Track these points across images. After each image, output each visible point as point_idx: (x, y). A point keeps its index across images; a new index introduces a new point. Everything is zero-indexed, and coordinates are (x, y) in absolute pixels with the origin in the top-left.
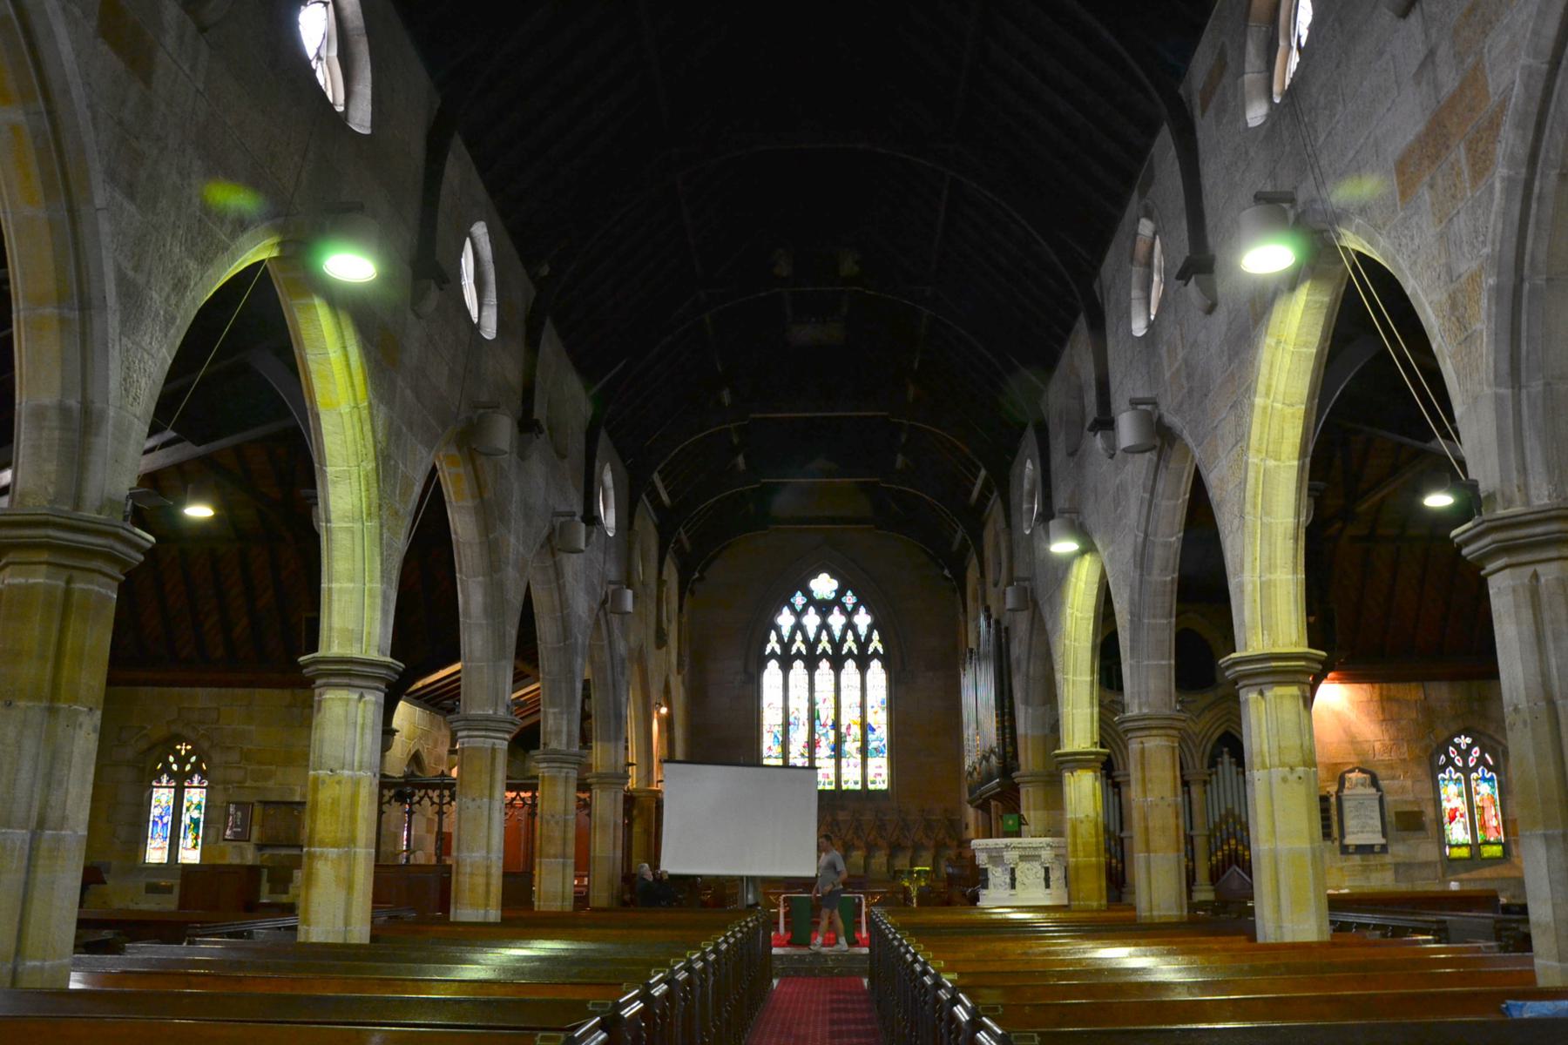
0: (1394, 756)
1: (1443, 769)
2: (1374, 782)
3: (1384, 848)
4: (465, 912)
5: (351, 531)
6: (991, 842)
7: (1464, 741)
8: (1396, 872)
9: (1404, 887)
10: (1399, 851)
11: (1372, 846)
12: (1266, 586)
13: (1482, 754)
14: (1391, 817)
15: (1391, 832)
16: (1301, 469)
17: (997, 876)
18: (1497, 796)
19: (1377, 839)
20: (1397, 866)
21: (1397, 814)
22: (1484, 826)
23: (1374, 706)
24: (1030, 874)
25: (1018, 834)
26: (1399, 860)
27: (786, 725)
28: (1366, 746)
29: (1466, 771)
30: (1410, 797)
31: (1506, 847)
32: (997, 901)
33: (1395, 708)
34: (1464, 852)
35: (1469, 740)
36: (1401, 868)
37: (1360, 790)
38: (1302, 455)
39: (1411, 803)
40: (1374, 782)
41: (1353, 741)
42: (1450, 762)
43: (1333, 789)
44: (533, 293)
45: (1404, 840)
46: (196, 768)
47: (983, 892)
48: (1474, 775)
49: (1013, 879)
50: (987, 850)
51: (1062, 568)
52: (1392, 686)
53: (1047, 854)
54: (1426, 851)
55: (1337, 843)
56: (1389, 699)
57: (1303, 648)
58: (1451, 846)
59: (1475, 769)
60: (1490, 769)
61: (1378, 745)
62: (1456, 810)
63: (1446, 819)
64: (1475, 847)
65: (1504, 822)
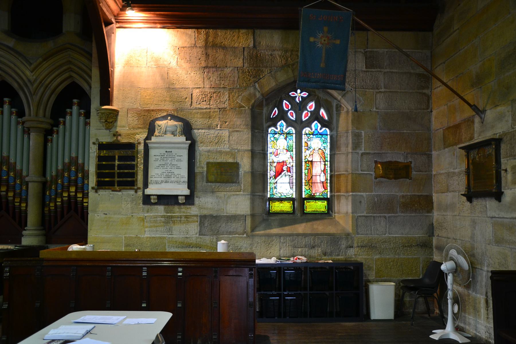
0: (213, 104)
2: (187, 130)
3: (189, 200)
7: (299, 95)
8: (201, 224)
11: (176, 196)
13: (317, 109)
15: (200, 183)
18: (328, 152)
19: (183, 190)
20: (203, 218)
21: (208, 163)
22: (311, 182)
23: (198, 52)
26: (205, 212)
28: (184, 94)
29: (299, 125)
30: (225, 148)
31: (329, 201)
33: (220, 54)
34: (286, 207)
35: (305, 94)
36: (210, 222)
37: (169, 138)
39: (227, 153)
41: (170, 87)
42: (282, 115)
43: (141, 136)
45: (213, 192)
48: (307, 130)
52: (220, 33)
55: (140, 193)
56: (215, 46)
58: (272, 199)
59: (308, 124)
60: (324, 123)
61: (196, 93)
62: (284, 163)
63: (271, 173)
64: (299, 202)
65: (331, 177)
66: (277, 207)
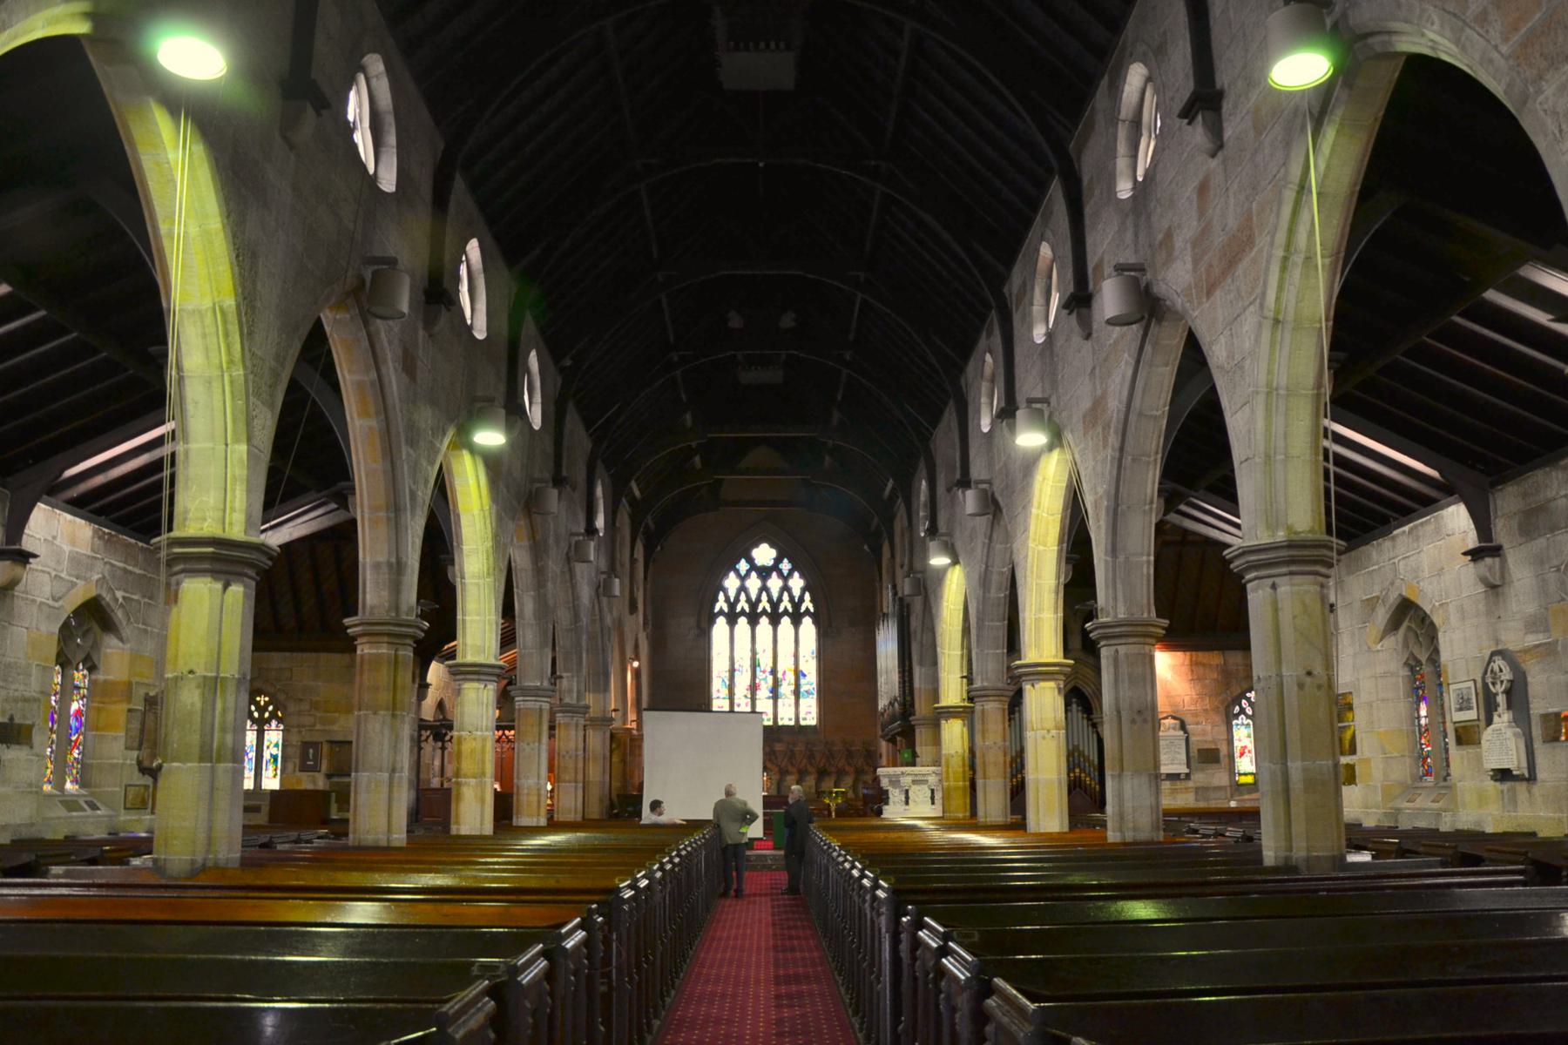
1: (1236, 716)
2: (1183, 726)
3: (1188, 776)
4: (524, 820)
5: (478, 585)
6: (891, 770)
9: (1202, 805)
10: (1199, 778)
12: (1038, 620)
14: (1194, 753)
15: (1193, 764)
16: (1060, 551)
17: (895, 795)
19: (1184, 770)
20: (1197, 789)
23: (1185, 669)
24: (920, 794)
25: (913, 764)
27: (732, 671)
28: (1179, 700)
30: (1209, 738)
32: (894, 812)
34: (1250, 779)
36: (1200, 791)
37: (1172, 732)
38: (1061, 542)
40: (1183, 726)
42: (1242, 711)
44: (560, 381)
46: (273, 715)
47: (885, 808)
49: (907, 798)
50: (888, 776)
51: (941, 574)
53: (932, 779)
54: (1220, 778)
57: (1060, 659)
61: (1187, 699)
62: (1244, 748)
63: (1237, 754)
66: (1243, 780)
